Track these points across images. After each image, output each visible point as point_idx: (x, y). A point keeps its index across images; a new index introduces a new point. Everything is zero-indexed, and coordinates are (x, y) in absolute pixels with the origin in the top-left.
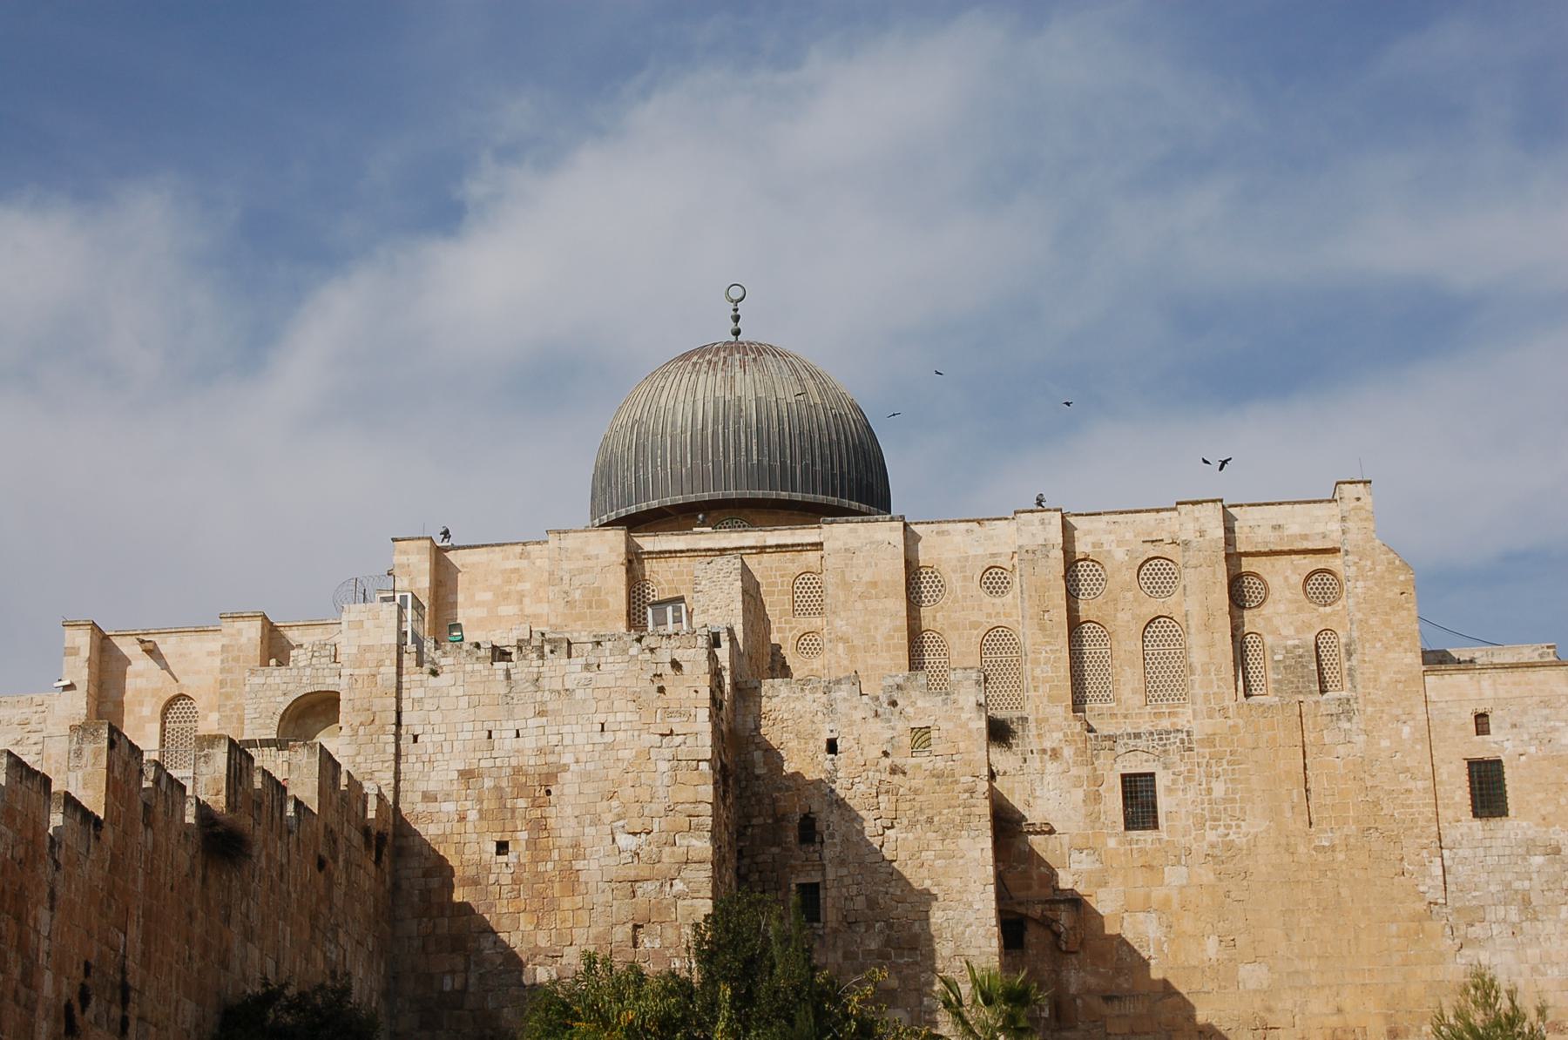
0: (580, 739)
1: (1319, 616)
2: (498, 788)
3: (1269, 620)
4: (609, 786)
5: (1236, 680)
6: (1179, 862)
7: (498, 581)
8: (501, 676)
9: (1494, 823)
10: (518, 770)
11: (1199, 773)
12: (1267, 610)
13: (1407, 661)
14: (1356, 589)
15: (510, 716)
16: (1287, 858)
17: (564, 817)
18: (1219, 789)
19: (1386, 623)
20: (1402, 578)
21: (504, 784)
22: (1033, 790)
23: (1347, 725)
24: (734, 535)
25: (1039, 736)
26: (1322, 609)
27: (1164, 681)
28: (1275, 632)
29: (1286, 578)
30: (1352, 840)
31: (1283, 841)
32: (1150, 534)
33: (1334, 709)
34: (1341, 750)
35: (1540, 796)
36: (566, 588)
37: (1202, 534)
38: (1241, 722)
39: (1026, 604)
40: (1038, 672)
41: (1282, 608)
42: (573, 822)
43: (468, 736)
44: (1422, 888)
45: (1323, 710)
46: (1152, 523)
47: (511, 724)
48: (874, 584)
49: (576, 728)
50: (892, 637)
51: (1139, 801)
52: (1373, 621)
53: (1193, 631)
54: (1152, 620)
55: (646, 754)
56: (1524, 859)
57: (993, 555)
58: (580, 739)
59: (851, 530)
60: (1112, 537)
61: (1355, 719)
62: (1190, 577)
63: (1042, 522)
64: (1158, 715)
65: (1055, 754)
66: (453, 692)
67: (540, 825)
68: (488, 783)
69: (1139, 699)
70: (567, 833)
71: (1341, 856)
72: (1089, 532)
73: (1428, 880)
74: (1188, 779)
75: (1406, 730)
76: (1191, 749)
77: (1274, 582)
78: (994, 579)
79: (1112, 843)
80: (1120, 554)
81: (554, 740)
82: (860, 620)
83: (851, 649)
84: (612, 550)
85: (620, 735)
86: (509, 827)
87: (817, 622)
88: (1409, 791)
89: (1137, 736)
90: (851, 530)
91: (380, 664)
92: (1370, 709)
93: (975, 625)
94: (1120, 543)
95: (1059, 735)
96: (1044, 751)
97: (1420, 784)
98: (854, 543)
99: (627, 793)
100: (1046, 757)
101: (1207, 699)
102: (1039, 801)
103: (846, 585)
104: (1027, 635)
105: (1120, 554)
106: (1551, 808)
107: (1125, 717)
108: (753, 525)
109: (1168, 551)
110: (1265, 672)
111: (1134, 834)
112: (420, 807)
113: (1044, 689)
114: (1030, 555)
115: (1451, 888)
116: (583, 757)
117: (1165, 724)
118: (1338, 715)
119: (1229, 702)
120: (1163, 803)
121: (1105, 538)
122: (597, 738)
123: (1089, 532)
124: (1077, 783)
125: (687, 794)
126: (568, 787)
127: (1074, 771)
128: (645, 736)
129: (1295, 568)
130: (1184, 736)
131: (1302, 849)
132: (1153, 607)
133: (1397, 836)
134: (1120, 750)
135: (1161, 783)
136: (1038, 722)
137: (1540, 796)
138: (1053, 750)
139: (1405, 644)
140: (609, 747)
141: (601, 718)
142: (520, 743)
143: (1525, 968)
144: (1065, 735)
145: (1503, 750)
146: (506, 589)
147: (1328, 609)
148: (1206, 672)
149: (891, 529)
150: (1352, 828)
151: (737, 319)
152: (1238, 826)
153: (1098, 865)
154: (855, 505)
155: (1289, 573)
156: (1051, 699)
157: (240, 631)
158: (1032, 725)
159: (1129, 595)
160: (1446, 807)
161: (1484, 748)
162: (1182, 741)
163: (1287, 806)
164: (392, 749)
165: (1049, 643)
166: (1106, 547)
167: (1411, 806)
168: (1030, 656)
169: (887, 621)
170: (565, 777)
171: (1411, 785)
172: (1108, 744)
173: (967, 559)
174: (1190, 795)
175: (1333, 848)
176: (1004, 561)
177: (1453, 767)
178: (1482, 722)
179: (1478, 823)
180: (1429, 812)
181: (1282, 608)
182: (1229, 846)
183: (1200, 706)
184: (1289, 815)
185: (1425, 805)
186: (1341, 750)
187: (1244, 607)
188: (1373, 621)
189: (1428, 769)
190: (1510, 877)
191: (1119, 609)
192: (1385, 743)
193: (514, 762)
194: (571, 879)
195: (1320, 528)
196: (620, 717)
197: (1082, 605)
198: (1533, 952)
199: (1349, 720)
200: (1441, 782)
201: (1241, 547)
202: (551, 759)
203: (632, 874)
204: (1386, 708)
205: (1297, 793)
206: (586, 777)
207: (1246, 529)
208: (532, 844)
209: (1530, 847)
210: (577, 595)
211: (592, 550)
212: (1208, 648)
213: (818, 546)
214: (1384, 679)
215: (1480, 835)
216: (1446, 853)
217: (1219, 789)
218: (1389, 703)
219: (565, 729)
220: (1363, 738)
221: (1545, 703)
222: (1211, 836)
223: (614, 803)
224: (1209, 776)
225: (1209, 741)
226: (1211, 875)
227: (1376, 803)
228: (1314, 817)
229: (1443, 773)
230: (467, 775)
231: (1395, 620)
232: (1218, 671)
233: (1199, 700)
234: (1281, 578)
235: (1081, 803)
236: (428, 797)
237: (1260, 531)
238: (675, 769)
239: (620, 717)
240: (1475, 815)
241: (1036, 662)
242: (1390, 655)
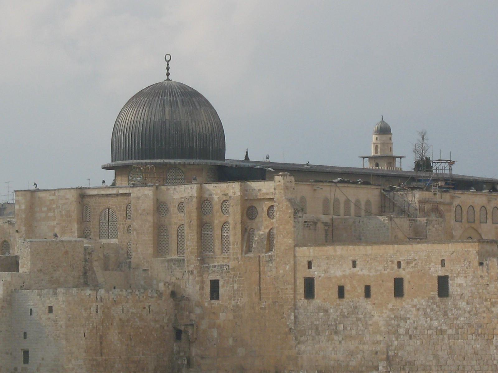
9: (311, 300)
13: (290, 242)
18: (236, 286)
20: (290, 211)
33: (267, 259)
34: (269, 274)
35: (324, 291)
38: (242, 263)
44: (288, 323)
48: (144, 210)
52: (281, 227)
53: (231, 229)
57: (181, 198)
71: (267, 311)
75: (288, 267)
83: (137, 234)
88: (287, 289)
95: (193, 266)
96: (189, 271)
97: (290, 286)
101: (233, 255)
111: (213, 301)
120: (221, 291)
130: (227, 267)
131: (257, 308)
135: (221, 283)
143: (314, 352)
145: (314, 275)
149: (150, 190)
152: (241, 300)
156: (191, 253)
158: (186, 262)
161: (309, 273)
171: (287, 287)
172: (206, 269)
179: (306, 301)
180: (292, 296)
182: (237, 306)
184: (254, 296)
188: (281, 227)
189: (293, 281)
192: (281, 272)
198: (317, 346)
199: (272, 263)
205: (257, 288)
209: (319, 309)
217: (236, 286)
221: (328, 258)
222: (233, 303)
224: (233, 281)
225: (233, 269)
235: (198, 290)
242: (285, 240)
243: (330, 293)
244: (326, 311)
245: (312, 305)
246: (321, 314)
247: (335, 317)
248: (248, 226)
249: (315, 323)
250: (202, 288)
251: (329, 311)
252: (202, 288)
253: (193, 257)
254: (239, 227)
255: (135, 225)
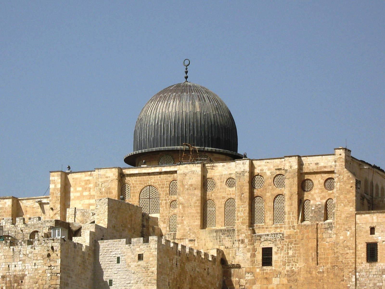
0: (30, 267)
1: (327, 194)
2: (10, 281)
3: (313, 195)
4: (35, 280)
5: (299, 215)
6: (277, 276)
7: (83, 184)
8: (11, 250)
9: (373, 264)
10: (15, 276)
11: (285, 247)
12: (312, 192)
13: (351, 210)
14: (337, 185)
15: (14, 261)
16: (309, 275)
18: (291, 253)
19: (345, 197)
20: (352, 182)
21: (12, 279)
22: (236, 253)
24: (153, 168)
25: (238, 235)
26: (329, 191)
27: (278, 217)
28: (314, 199)
29: (319, 181)
30: (329, 270)
31: (308, 270)
32: (278, 166)
33: (327, 226)
34: (328, 240)
36: (100, 188)
37: (291, 167)
38: (298, 230)
39: (237, 192)
41: (317, 191)
44: (349, 285)
45: (323, 226)
46: (279, 162)
47: (14, 263)
49: (29, 265)
50: (196, 203)
51: (267, 257)
52: (342, 196)
53: (286, 200)
54: (277, 196)
55: (44, 272)
56: (381, 276)
57: (230, 174)
58: (30, 267)
59: (186, 167)
60: (266, 167)
61: (333, 230)
64: (277, 228)
68: (8, 279)
69: (271, 222)
71: (325, 275)
72: (260, 166)
73: (351, 283)
74: (282, 250)
75: (348, 233)
76: (283, 240)
77: (315, 182)
78: (230, 182)
79: (258, 270)
80: (268, 173)
82: (187, 197)
83: (184, 207)
84: (114, 175)
85: (39, 266)
87: (175, 197)
88: (347, 253)
89: (268, 235)
90: (186, 167)
92: (338, 226)
93: (223, 198)
94: (269, 169)
95: (244, 235)
96: (239, 240)
97: (351, 251)
98: (186, 171)
99: (40, 282)
100: (240, 242)
101: (289, 224)
102: (237, 257)
103: (183, 186)
107: (267, 228)
108: (159, 163)
109: (283, 172)
110: (309, 214)
111: (265, 267)
113: (240, 220)
114: (240, 174)
115: (358, 285)
116: (30, 273)
117: (278, 231)
118: (328, 228)
119: (295, 224)
120: (274, 257)
122: (33, 267)
123: (260, 166)
124: (249, 251)
125: (54, 282)
126: (27, 280)
127: (248, 247)
128: (45, 267)
129: (322, 178)
130: (281, 235)
131: (314, 273)
132: (278, 191)
133: (343, 268)
134: (262, 240)
135: (274, 250)
136: (238, 231)
138: (242, 240)
139: (351, 204)
140: (36, 269)
141: (35, 261)
144: (246, 235)
145: (377, 239)
146: (86, 186)
147: (331, 191)
148: (289, 214)
150: (329, 265)
151: (186, 72)
152: (296, 265)
153: (253, 278)
155: (320, 179)
157: (5, 203)
158: (236, 232)
159: (270, 187)
160: (359, 258)
161: (372, 239)
162: (281, 237)
163: (310, 258)
165: (243, 204)
166: (264, 171)
167: (348, 258)
168: (237, 209)
169: (195, 197)
170: (26, 278)
171: (348, 251)
172: (258, 238)
173: (222, 175)
174: (282, 255)
175: (323, 272)
176: (233, 176)
177: (362, 245)
178: (372, 230)
179: (368, 264)
180: (353, 260)
181: (317, 191)
182: (292, 271)
183: (287, 225)
184: (311, 261)
185: (352, 258)
187: (304, 191)
188: (342, 196)
189: (354, 246)
190: (376, 281)
191: (266, 192)
192: (341, 238)
193: (14, 274)
195: (330, 164)
197: (255, 191)
199: (331, 230)
200: (358, 251)
201: (305, 170)
202: (23, 273)
204: (343, 226)
205: (314, 254)
206: (31, 278)
207: (307, 165)
210: (103, 190)
211: (108, 175)
212: (290, 206)
213: (175, 172)
214: (343, 216)
215: (368, 268)
216: (357, 274)
217: (291, 253)
218: (344, 224)
219: (26, 265)
220: (335, 236)
222: (288, 268)
223: (37, 285)
224: (288, 248)
225: (289, 237)
226: (286, 281)
227: (338, 257)
228: (319, 262)
229: (359, 247)
231: (348, 196)
232: (293, 214)
233: (287, 223)
234: (318, 181)
235: (249, 257)
237: (311, 165)
238: (51, 276)
240: (367, 261)
241: (239, 211)
242: (346, 208)
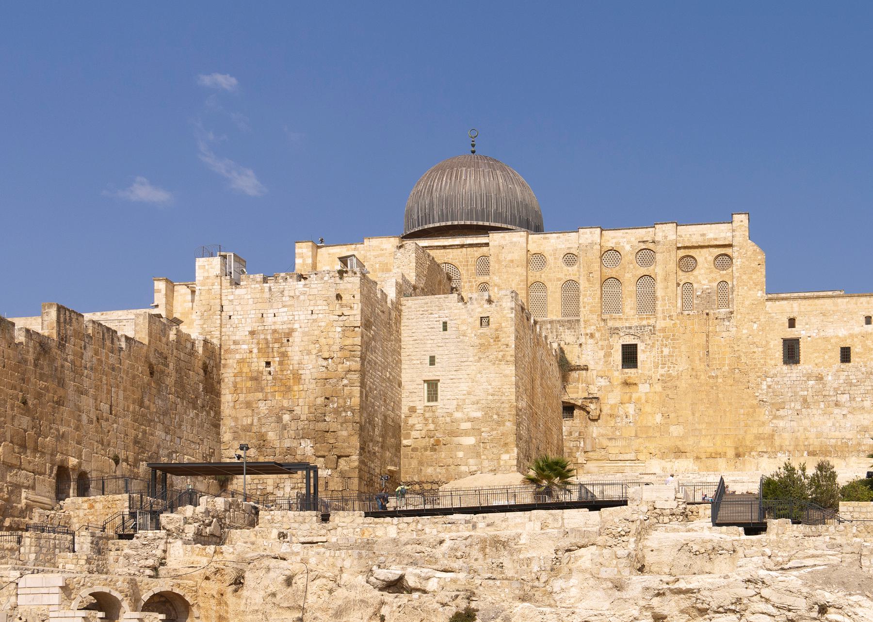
0: (302, 317)
9: (793, 366)
11: (658, 344)
17: (295, 351)
18: (666, 351)
21: (269, 337)
23: (728, 323)
31: (694, 373)
34: (724, 334)
40: (586, 300)
42: (299, 353)
43: (253, 316)
49: (300, 313)
51: (630, 356)
53: (658, 281)
55: (331, 324)
57: (569, 248)
58: (302, 317)
62: (658, 257)
63: (591, 233)
64: (641, 319)
65: (592, 336)
66: (246, 297)
67: (284, 355)
68: (262, 336)
69: (632, 312)
70: (296, 358)
78: (570, 258)
80: (628, 248)
81: (291, 318)
85: (320, 316)
86: (271, 355)
89: (630, 328)
91: (213, 285)
93: (559, 279)
94: (628, 242)
95: (593, 327)
97: (760, 349)
99: (323, 341)
101: (663, 312)
104: (583, 284)
105: (628, 248)
106: (820, 360)
112: (232, 347)
116: (303, 325)
117: (645, 323)
120: (641, 357)
121: (621, 240)
122: (309, 317)
126: (296, 338)
127: (600, 343)
132: (643, 271)
137: (816, 355)
140: (315, 321)
142: (279, 318)
148: (664, 300)
154: (509, 227)
156: (591, 312)
158: (582, 323)
160: (771, 359)
163: (697, 358)
164: (218, 322)
168: (583, 293)
170: (295, 334)
171: (755, 350)
175: (717, 377)
176: (573, 251)
179: (785, 367)
184: (697, 362)
186: (724, 334)
192: (745, 331)
193: (273, 327)
194: (297, 377)
196: (320, 308)
202: (289, 326)
203: (324, 376)
206: (305, 334)
208: (281, 363)
209: (809, 377)
217: (666, 351)
219: (296, 313)
220: (735, 329)
224: (662, 345)
225: (663, 330)
227: (739, 357)
230: (252, 333)
236: (235, 343)
239: (320, 308)
241: (585, 295)
243: (826, 357)
244: (820, 378)
245: (795, 371)
246: (811, 383)
247: (836, 386)
248: (681, 280)
249: (802, 393)
250: (608, 355)
251: (825, 379)
252: (608, 355)
253: (595, 317)
254: (673, 277)
255: (495, 279)
